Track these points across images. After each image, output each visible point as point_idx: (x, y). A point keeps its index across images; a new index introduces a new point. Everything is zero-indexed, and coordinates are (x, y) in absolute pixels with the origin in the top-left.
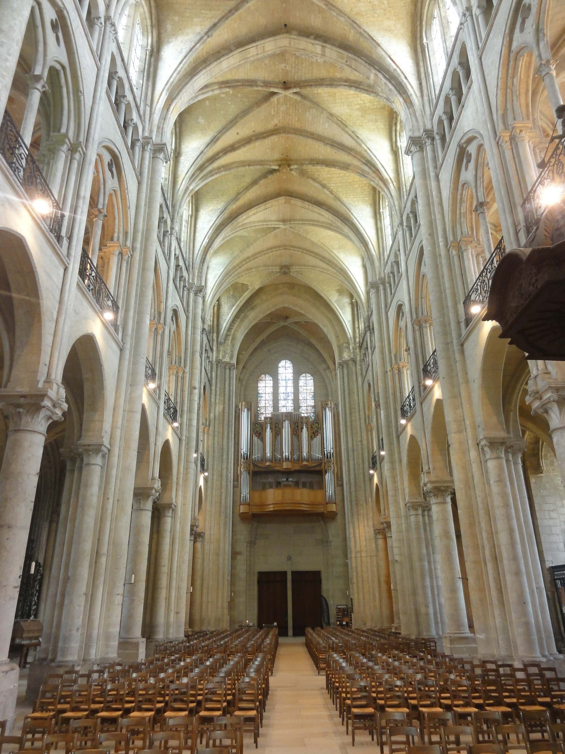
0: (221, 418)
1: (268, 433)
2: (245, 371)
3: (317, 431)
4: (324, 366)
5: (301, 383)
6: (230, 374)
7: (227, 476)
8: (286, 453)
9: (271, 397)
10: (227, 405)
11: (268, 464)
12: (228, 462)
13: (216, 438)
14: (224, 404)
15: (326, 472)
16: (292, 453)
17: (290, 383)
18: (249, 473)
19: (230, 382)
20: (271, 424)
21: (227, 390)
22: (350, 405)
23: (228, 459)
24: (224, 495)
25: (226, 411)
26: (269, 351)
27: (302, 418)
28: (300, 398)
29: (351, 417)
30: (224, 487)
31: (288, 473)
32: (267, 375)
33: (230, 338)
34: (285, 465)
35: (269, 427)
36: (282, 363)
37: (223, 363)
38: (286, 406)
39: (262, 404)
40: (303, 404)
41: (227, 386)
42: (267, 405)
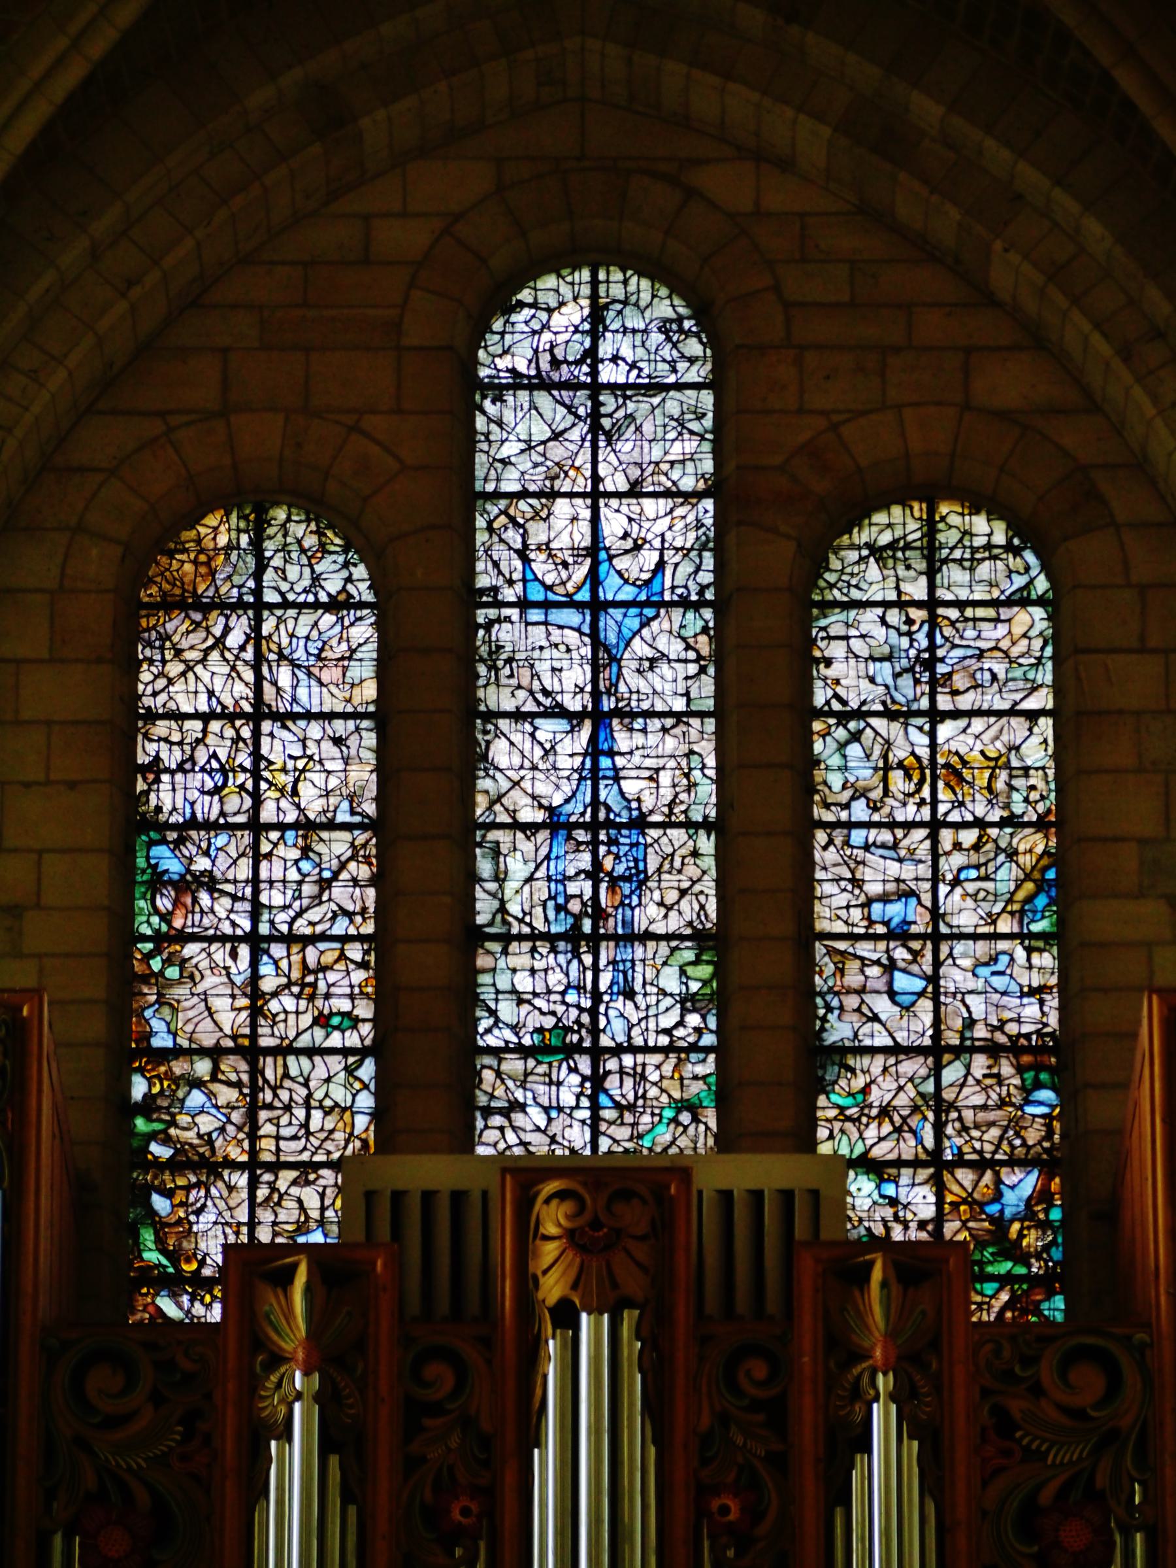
9: (354, 894)
17: (668, 666)
28: (834, 907)
36: (548, 319)
40: (873, 1013)
42: (290, 1016)
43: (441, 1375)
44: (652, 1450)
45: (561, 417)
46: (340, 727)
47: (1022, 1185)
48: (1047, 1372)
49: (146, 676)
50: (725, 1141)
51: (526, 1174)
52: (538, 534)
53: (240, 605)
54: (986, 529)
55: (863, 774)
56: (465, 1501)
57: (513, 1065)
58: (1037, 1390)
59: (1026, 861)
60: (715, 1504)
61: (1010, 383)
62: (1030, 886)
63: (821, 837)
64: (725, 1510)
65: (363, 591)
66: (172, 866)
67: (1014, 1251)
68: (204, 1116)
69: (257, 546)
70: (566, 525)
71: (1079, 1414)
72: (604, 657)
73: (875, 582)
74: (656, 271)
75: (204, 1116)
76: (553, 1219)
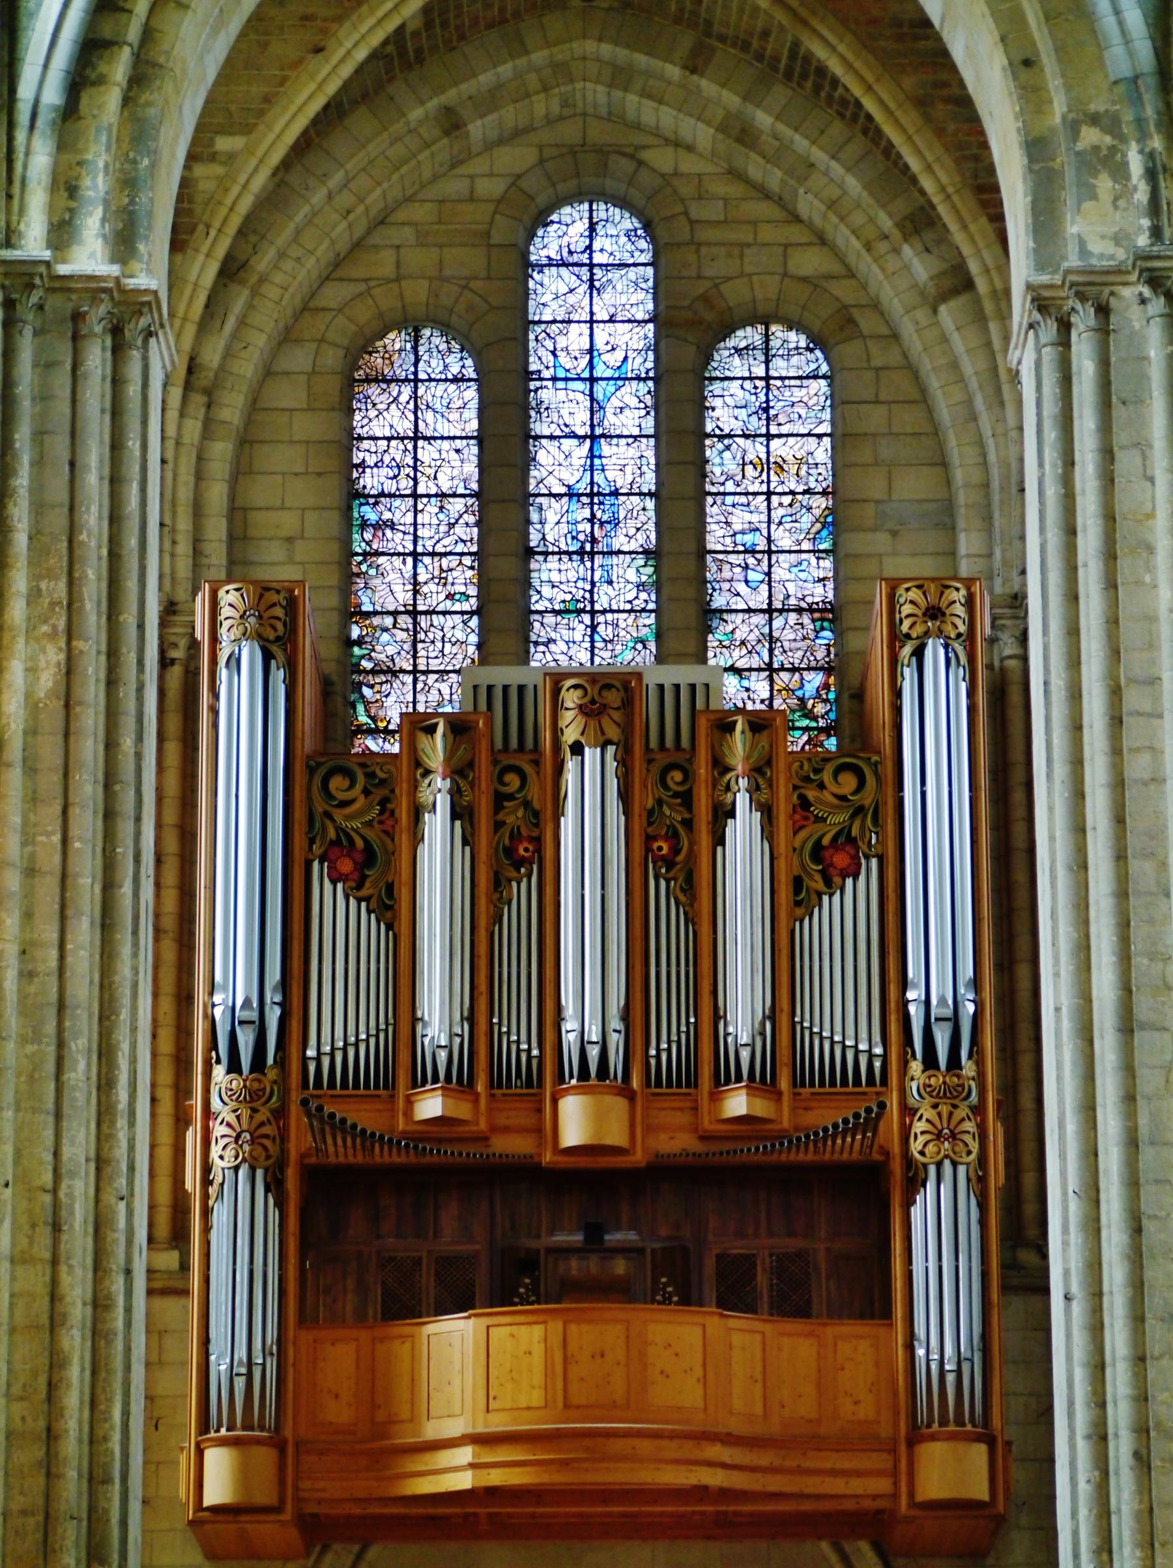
0: (50, 751)
1: (437, 859)
2: (239, 299)
3: (846, 839)
4: (920, 267)
5: (727, 408)
6: (117, 382)
7: (100, 1225)
8: (587, 1010)
9: (467, 531)
10: (92, 647)
11: (431, 1106)
12: (105, 1113)
14: (70, 634)
15: (914, 1181)
16: (636, 1015)
17: (629, 409)
18: (275, 1186)
19: (116, 446)
20: (459, 772)
21: (94, 518)
22: (1114, 653)
23: (105, 1084)
24: (76, 1374)
25: (92, 691)
27: (724, 725)
28: (716, 537)
29: (1116, 751)
30: (78, 1310)
31: (593, 1182)
32: (431, 338)
33: (119, 68)
34: (576, 1121)
35: (443, 803)
36: (566, 230)
37: (63, 285)
38: (593, 615)
39: (388, 587)
40: (735, 589)
41: (93, 480)
42: (434, 597)
43: (513, 781)
44: (623, 818)
45: (574, 282)
46: (459, 444)
47: (815, 680)
48: (827, 776)
49: (357, 417)
50: (660, 659)
51: (557, 679)
52: (562, 342)
53: (409, 381)
54: (796, 339)
55: (732, 467)
56: (526, 844)
57: (550, 619)
58: (822, 786)
59: (817, 512)
60: (655, 845)
62: (818, 526)
63: (710, 500)
64: (660, 848)
65: (470, 373)
66: (372, 516)
67: (809, 715)
68: (390, 646)
69: (415, 349)
70: (577, 338)
71: (843, 798)
73: (738, 367)
74: (623, 203)
75: (390, 646)
76: (571, 698)
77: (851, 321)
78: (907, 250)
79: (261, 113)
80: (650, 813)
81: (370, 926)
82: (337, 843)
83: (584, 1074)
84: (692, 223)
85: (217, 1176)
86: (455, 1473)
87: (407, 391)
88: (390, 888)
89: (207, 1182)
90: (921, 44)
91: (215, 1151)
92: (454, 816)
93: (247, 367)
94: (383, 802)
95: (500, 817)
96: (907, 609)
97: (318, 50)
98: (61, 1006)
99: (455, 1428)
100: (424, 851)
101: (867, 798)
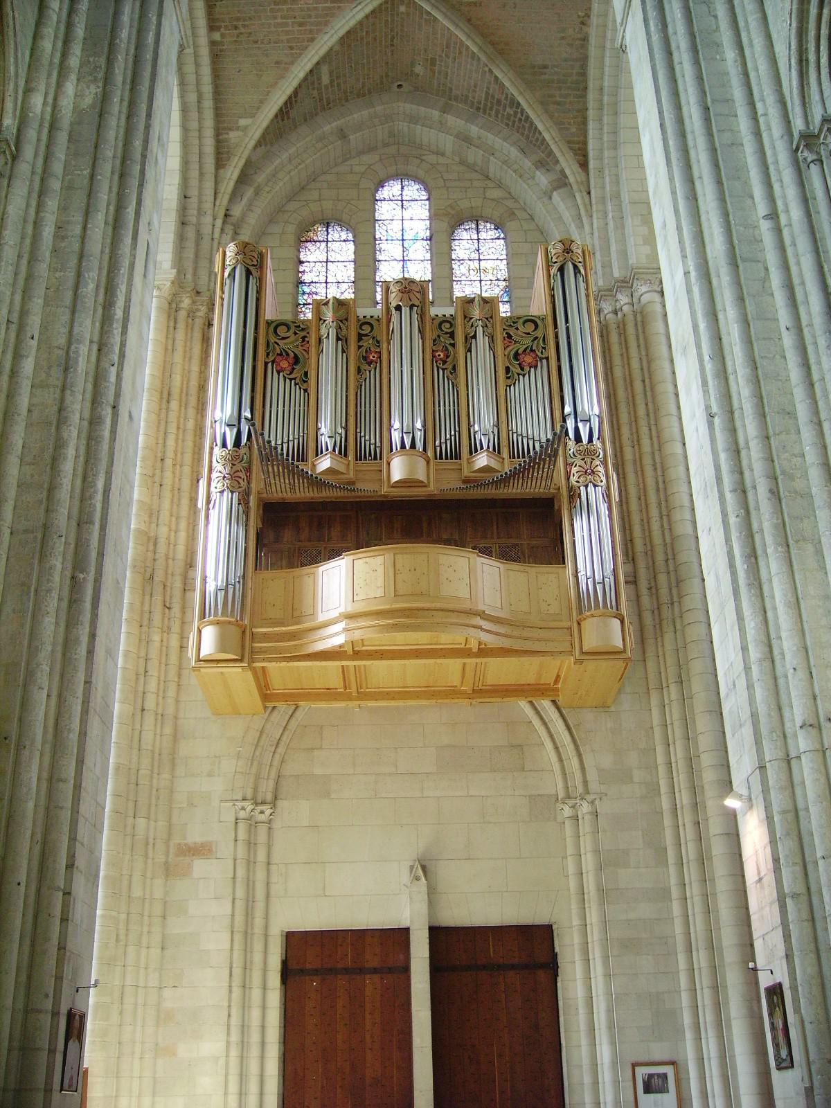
1: (329, 367)
4: (543, 179)
13: (52, 204)
18: (244, 501)
23: (108, 305)
26: (342, 135)
36: (391, 189)
44: (421, 341)
45: (395, 206)
46: (345, 264)
49: (302, 254)
52: (390, 227)
53: (324, 241)
56: (373, 354)
58: (517, 329)
59: (502, 287)
60: (437, 354)
61: (495, 193)
62: (502, 292)
63: (455, 283)
64: (439, 355)
65: (350, 237)
66: (306, 289)
69: (327, 231)
71: (528, 334)
72: (404, 249)
73: (465, 235)
77: (514, 213)
78: (538, 173)
79: (258, 108)
80: (434, 341)
81: (297, 393)
82: (281, 354)
83: (403, 446)
84: (444, 180)
85: (213, 498)
86: (335, 637)
87: (324, 244)
88: (306, 374)
89: (208, 502)
90: (543, 77)
91: (213, 484)
92: (338, 339)
93: (253, 219)
94: (303, 338)
95: (361, 344)
96: (553, 252)
97: (282, 77)
98: (81, 256)
99: (334, 614)
100: (323, 357)
101: (539, 333)
